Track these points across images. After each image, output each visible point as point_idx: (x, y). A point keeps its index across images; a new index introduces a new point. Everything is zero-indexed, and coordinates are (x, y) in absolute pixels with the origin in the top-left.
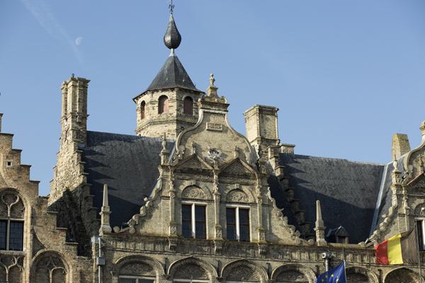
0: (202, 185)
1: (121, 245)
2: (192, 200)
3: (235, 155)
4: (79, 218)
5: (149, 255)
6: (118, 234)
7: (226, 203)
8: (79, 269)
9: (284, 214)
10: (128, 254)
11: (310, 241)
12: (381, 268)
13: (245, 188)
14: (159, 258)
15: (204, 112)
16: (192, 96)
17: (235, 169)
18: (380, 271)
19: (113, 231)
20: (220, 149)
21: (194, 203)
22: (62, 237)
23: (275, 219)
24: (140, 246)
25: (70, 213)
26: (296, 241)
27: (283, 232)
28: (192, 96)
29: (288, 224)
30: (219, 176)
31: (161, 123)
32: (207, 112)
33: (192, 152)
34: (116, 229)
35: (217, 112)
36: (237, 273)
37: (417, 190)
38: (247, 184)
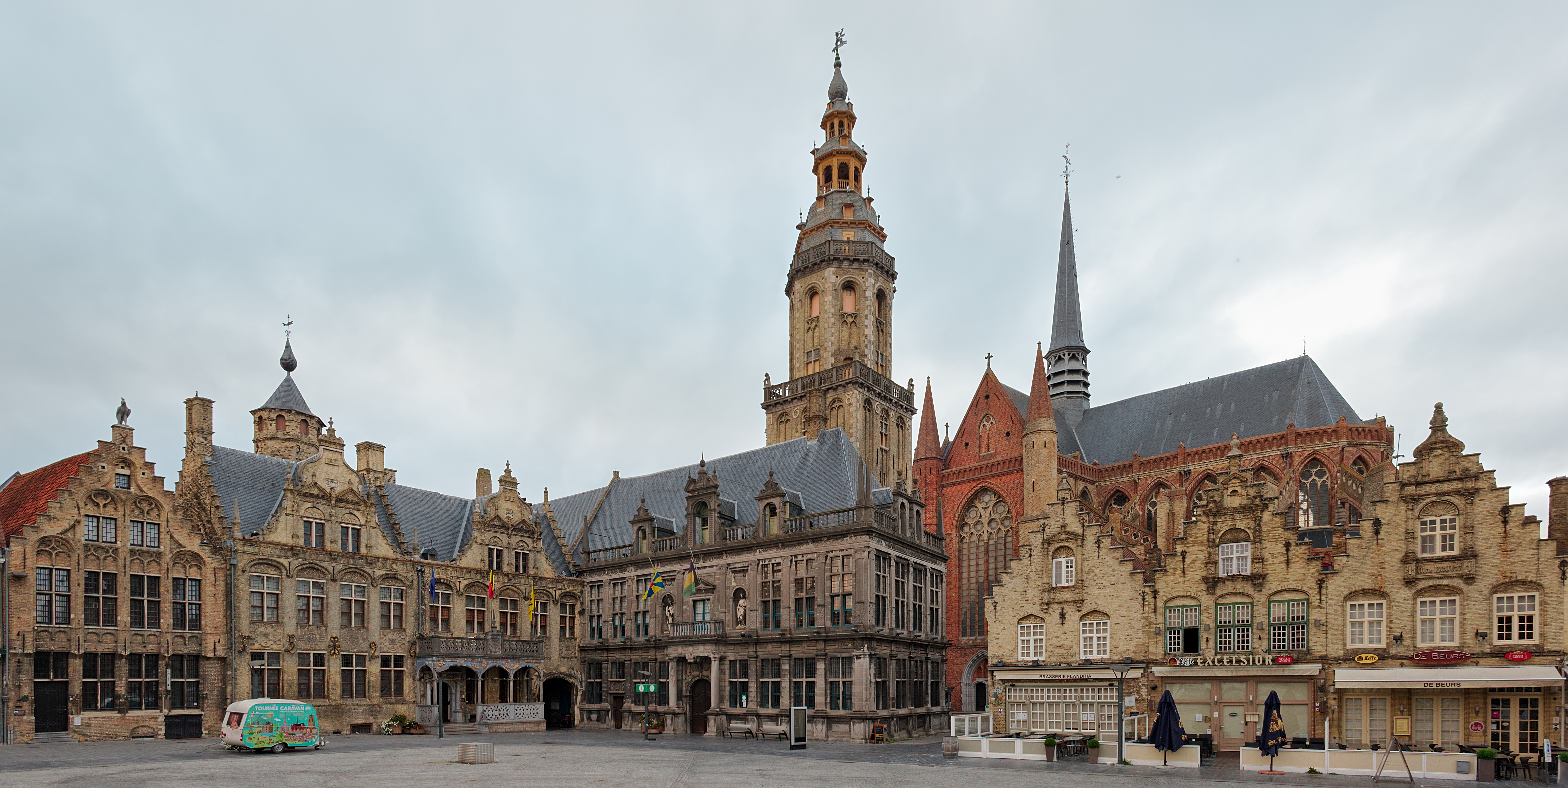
1: (248, 549)
4: (209, 522)
6: (248, 541)
8: (213, 566)
10: (257, 557)
16: (308, 419)
21: (315, 521)
22: (197, 541)
25: (199, 516)
28: (308, 419)
31: (279, 439)
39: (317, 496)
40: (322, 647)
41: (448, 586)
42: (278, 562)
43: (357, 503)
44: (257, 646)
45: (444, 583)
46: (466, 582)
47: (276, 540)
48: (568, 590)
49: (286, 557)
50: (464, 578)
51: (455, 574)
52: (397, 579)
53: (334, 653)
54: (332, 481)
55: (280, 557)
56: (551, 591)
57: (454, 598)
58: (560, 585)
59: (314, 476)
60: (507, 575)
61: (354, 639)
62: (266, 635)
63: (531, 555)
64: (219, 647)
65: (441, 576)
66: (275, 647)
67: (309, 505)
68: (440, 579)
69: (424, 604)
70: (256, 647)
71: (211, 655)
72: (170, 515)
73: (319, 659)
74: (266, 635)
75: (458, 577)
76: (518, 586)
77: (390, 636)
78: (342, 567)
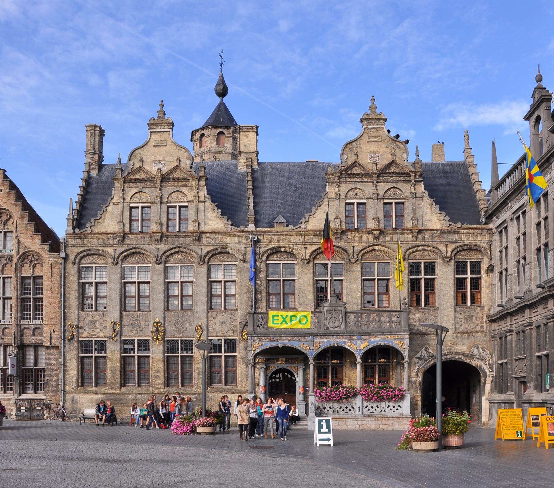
0: (146, 190)
1: (79, 242)
2: (137, 203)
3: (176, 163)
5: (102, 248)
7: (167, 202)
8: (50, 262)
9: (218, 207)
11: (242, 228)
12: (307, 246)
13: (182, 189)
14: (110, 250)
15: (151, 132)
17: (176, 175)
18: (306, 248)
19: (74, 232)
20: (164, 160)
23: (211, 212)
24: (94, 241)
26: (230, 228)
27: (214, 221)
29: (222, 215)
30: (162, 181)
32: (154, 132)
33: (137, 165)
34: (77, 231)
35: (163, 130)
36: (176, 257)
37: (350, 176)
38: (186, 186)
39: (143, 180)
40: (147, 334)
41: (291, 255)
42: (103, 251)
43: (185, 179)
44: (85, 334)
45: (285, 252)
46: (314, 247)
47: (103, 230)
48: (467, 242)
49: (112, 245)
50: (311, 244)
51: (299, 239)
52: (228, 253)
53: (157, 339)
54: (159, 162)
55: (104, 245)
56: (440, 246)
57: (298, 268)
58: (453, 238)
59: (142, 160)
60: (370, 232)
61: (179, 323)
62: (93, 324)
63: (408, 205)
64: (55, 337)
65: (281, 244)
66: (101, 334)
67: (135, 190)
68: (279, 247)
69: (260, 279)
70: (84, 336)
71: (47, 344)
72: (19, 222)
73: (144, 345)
74: (93, 324)
75: (304, 243)
76: (388, 244)
77: (220, 317)
78: (167, 248)
